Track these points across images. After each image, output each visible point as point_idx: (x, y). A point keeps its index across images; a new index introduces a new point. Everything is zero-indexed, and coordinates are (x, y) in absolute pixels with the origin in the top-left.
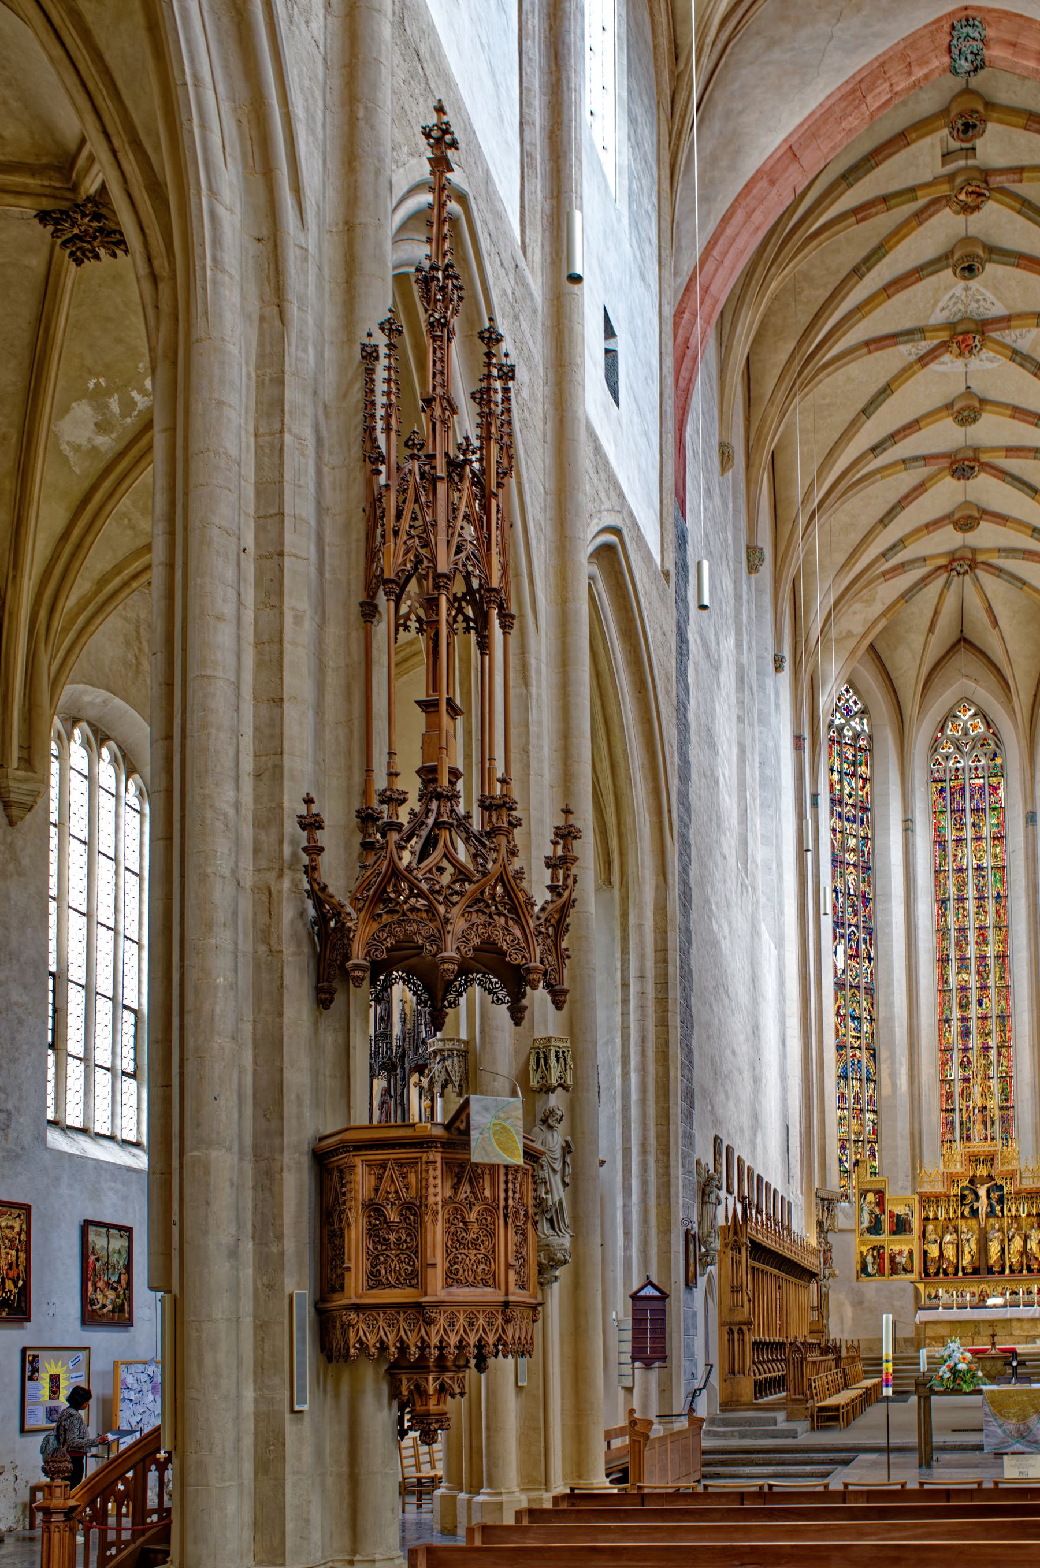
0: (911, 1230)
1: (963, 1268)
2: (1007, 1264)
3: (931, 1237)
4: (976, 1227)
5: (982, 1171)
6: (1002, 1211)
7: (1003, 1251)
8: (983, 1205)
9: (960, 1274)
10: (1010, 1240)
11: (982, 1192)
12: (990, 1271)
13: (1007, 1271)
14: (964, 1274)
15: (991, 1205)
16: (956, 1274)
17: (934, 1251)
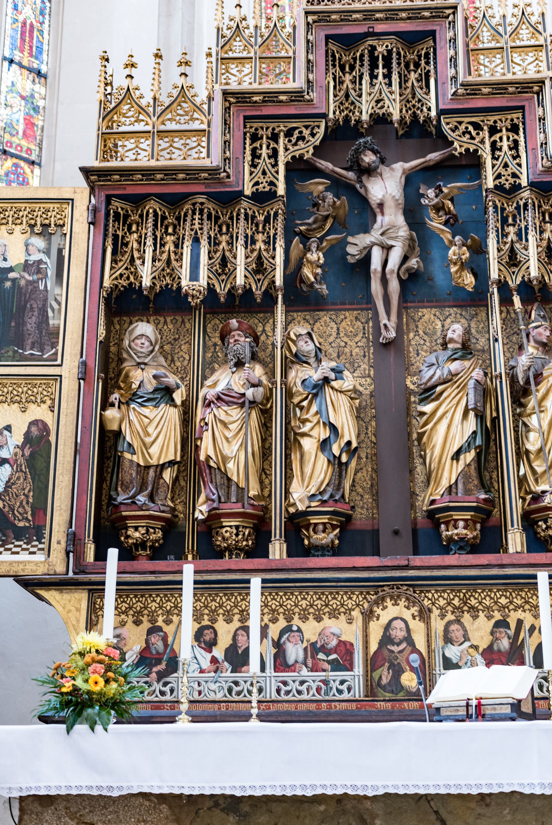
0: (50, 337)
1: (296, 524)
2: (515, 507)
3: (142, 378)
4: (356, 346)
5: (380, 97)
6: (477, 263)
7: (486, 448)
8: (386, 242)
9: (277, 550)
10: (520, 393)
11: (386, 187)
12: (428, 533)
13: (515, 540)
14: (297, 547)
15: (420, 238)
16: (259, 549)
17: (153, 433)
